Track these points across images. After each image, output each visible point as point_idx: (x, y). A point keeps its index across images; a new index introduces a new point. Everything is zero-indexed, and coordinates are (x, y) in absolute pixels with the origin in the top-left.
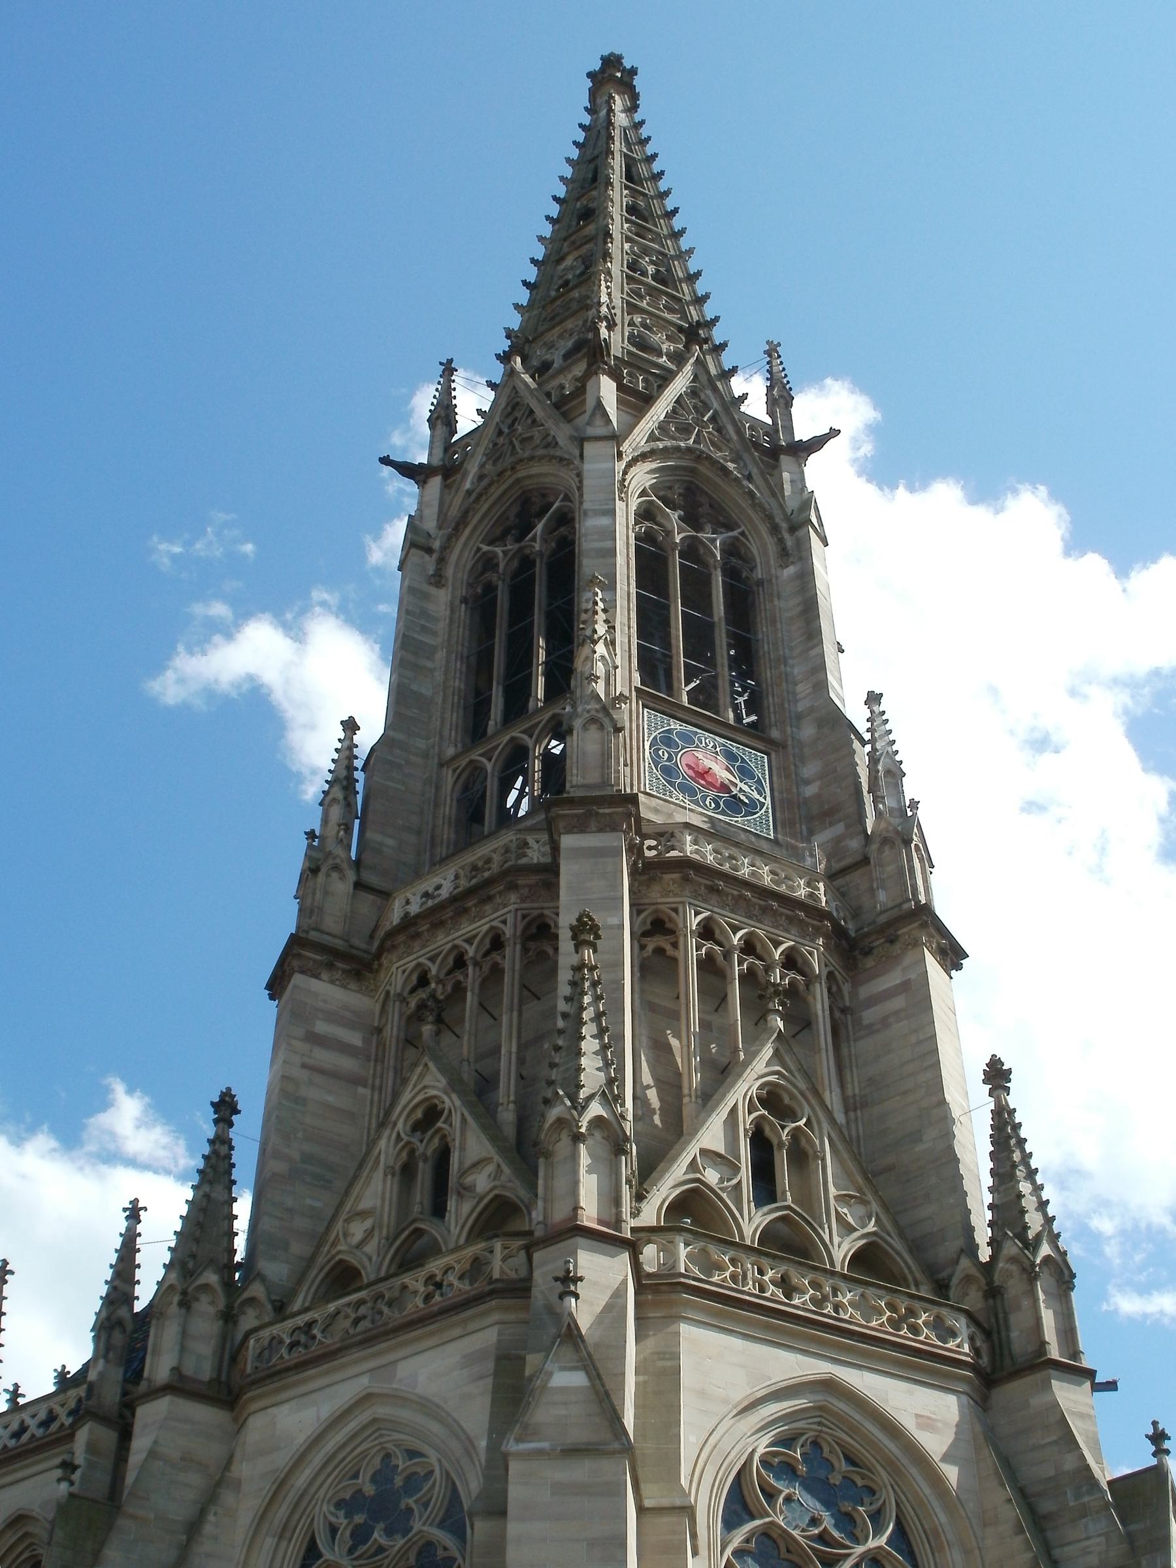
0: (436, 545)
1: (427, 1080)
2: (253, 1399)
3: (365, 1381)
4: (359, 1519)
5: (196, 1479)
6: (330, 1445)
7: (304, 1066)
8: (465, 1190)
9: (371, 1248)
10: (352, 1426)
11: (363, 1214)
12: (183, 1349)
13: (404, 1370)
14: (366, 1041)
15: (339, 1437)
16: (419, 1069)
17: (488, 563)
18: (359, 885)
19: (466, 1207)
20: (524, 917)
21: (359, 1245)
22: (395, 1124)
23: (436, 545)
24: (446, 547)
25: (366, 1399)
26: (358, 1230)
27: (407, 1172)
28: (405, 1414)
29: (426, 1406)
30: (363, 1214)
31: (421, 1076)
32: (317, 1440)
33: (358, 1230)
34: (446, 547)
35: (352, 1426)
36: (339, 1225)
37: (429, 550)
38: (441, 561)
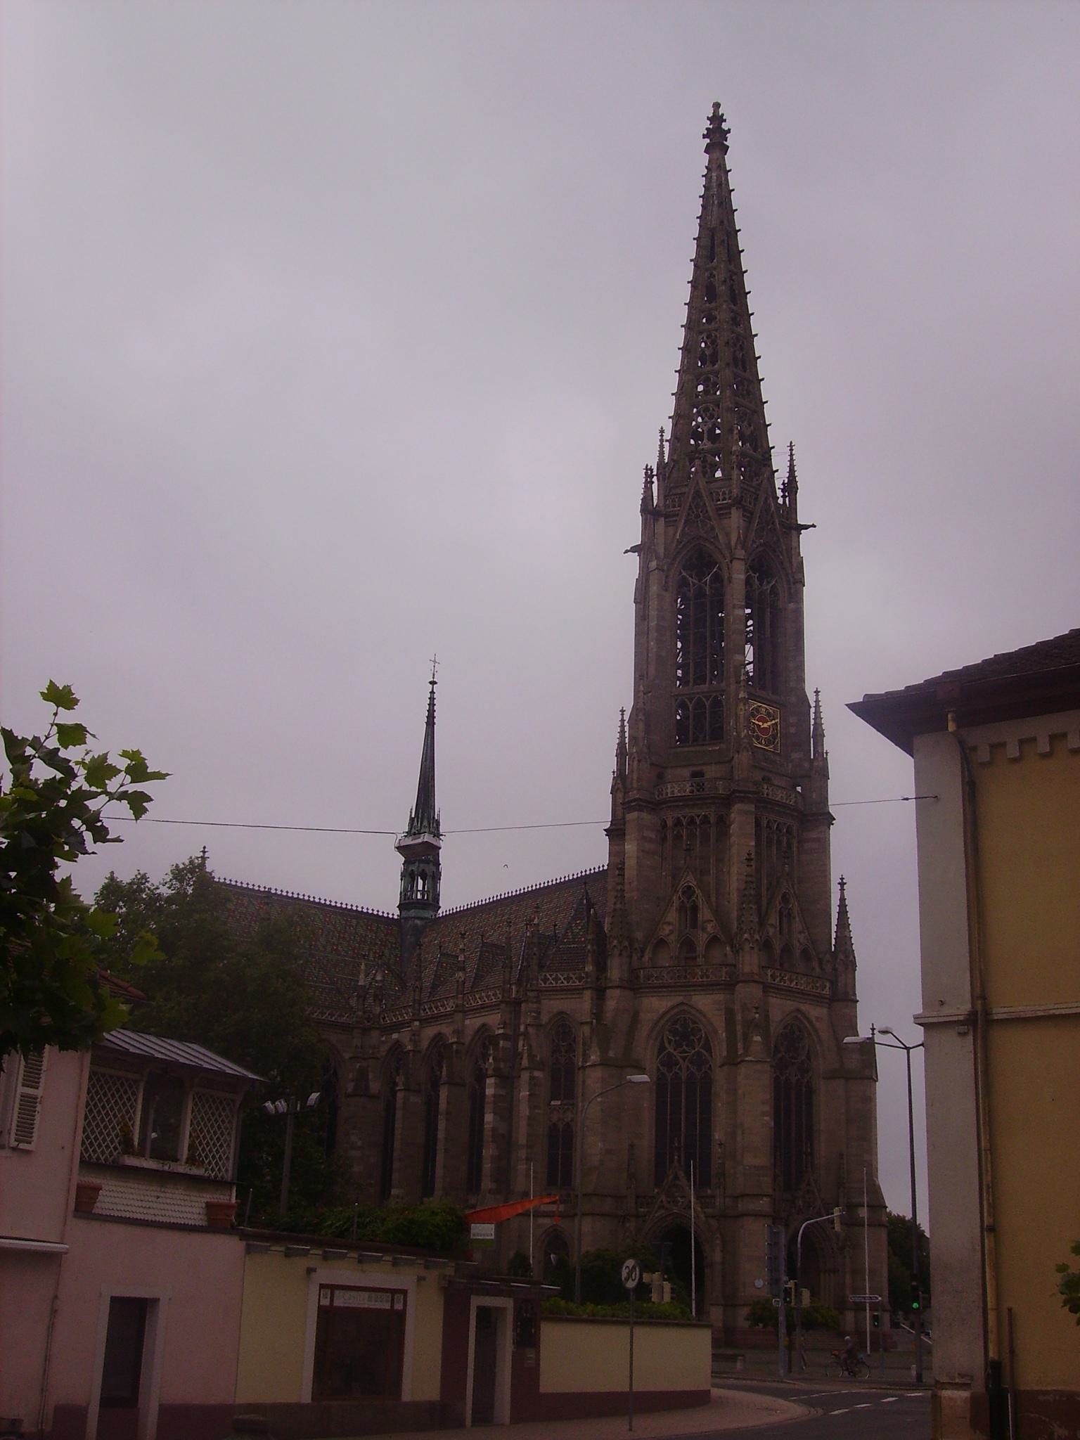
0: (665, 568)
1: (688, 878)
2: (642, 992)
3: (681, 998)
4: (677, 1038)
6: (669, 1016)
7: (643, 851)
8: (704, 929)
9: (672, 937)
10: (676, 1010)
11: (669, 924)
13: (695, 998)
14: (656, 836)
15: (672, 1013)
16: (686, 873)
17: (683, 583)
18: (652, 764)
19: (706, 936)
20: (717, 814)
22: (678, 891)
23: (665, 568)
24: (669, 570)
25: (682, 1003)
26: (667, 929)
27: (682, 909)
28: (693, 1012)
29: (700, 1012)
30: (669, 924)
31: (687, 876)
32: (665, 1014)
33: (667, 929)
34: (669, 570)
35: (676, 1010)
36: (660, 925)
37: (663, 571)
38: (667, 577)
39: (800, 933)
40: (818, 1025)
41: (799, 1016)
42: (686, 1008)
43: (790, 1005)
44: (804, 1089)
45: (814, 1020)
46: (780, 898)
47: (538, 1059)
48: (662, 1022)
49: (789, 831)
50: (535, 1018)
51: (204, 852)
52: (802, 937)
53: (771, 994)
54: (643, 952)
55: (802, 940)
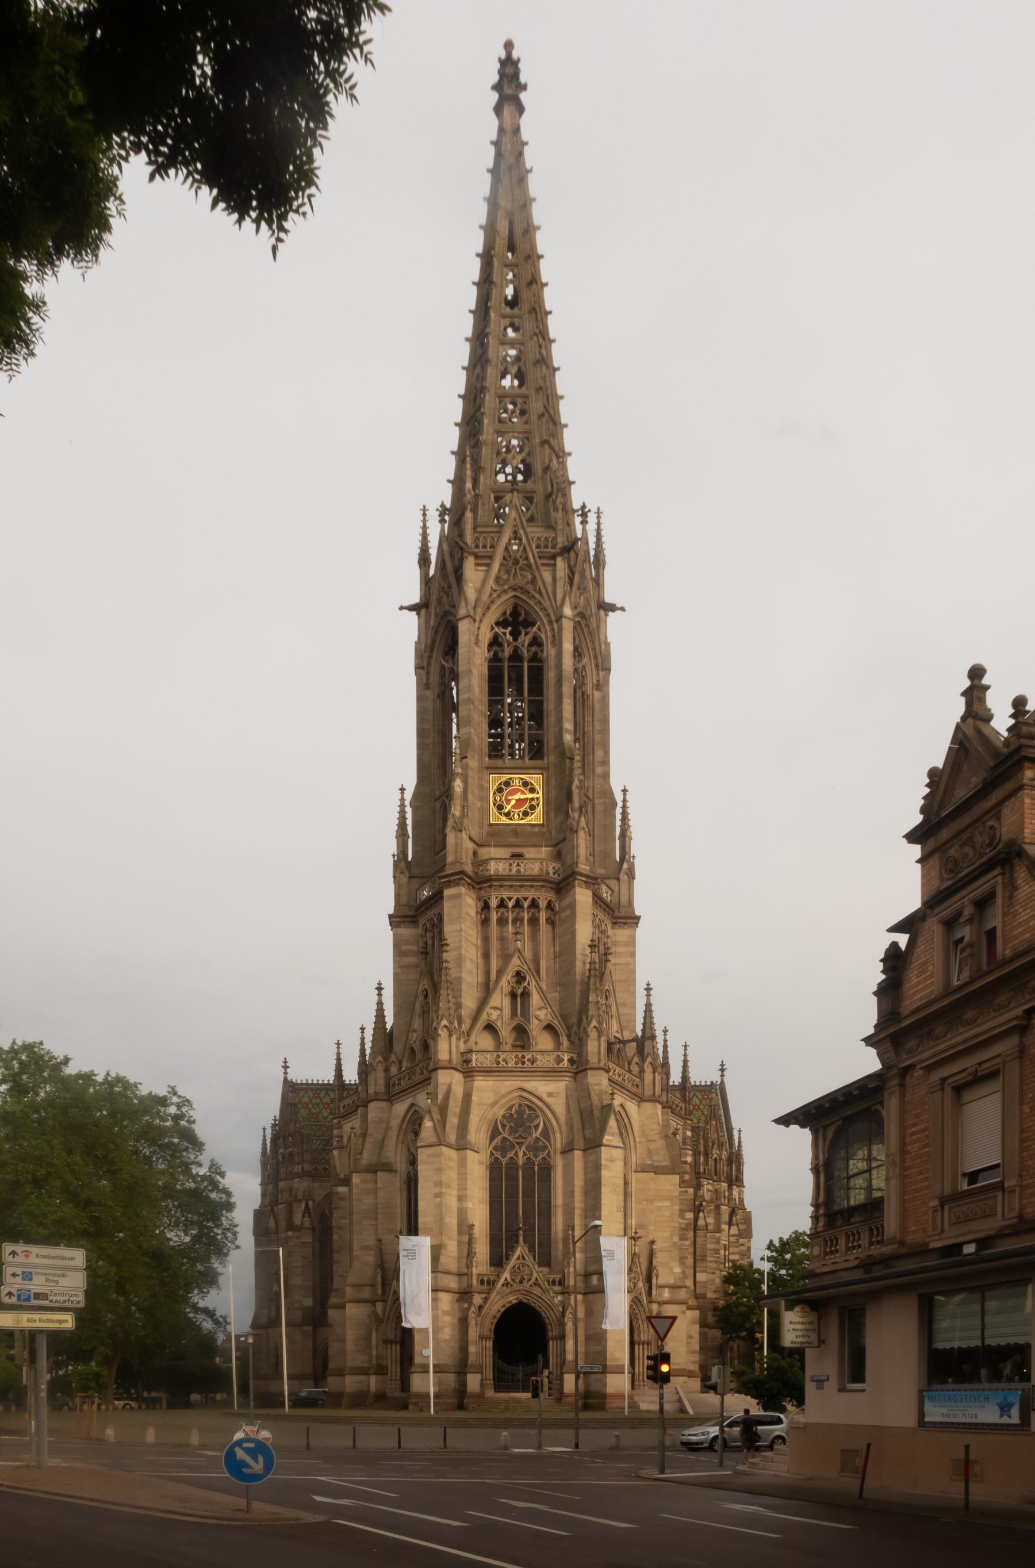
3: (411, 1099)
5: (384, 1126)
12: (375, 1084)
21: (415, 1042)
25: (412, 1105)
26: (415, 1035)
30: (414, 1031)
33: (415, 1035)
39: (540, 1009)
40: (550, 1101)
41: (525, 1094)
42: (417, 1108)
43: (509, 1084)
44: (536, 1168)
45: (545, 1097)
46: (509, 978)
47: (342, 1176)
48: (405, 1125)
49: (534, 904)
50: (338, 1142)
51: (285, 1062)
52: (542, 1014)
53: (477, 1078)
54: (400, 1062)
55: (542, 1017)
